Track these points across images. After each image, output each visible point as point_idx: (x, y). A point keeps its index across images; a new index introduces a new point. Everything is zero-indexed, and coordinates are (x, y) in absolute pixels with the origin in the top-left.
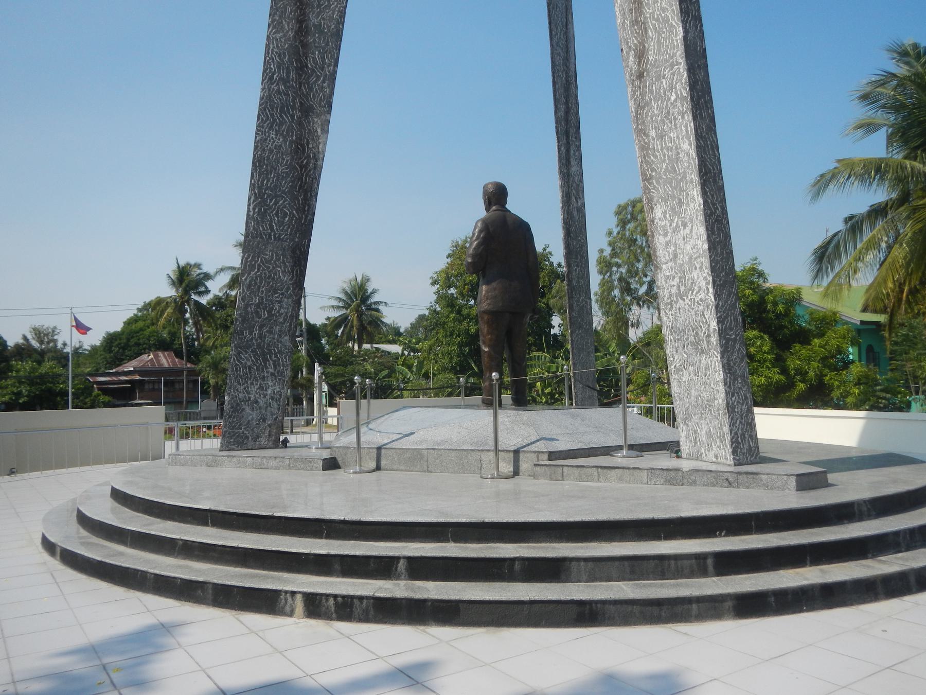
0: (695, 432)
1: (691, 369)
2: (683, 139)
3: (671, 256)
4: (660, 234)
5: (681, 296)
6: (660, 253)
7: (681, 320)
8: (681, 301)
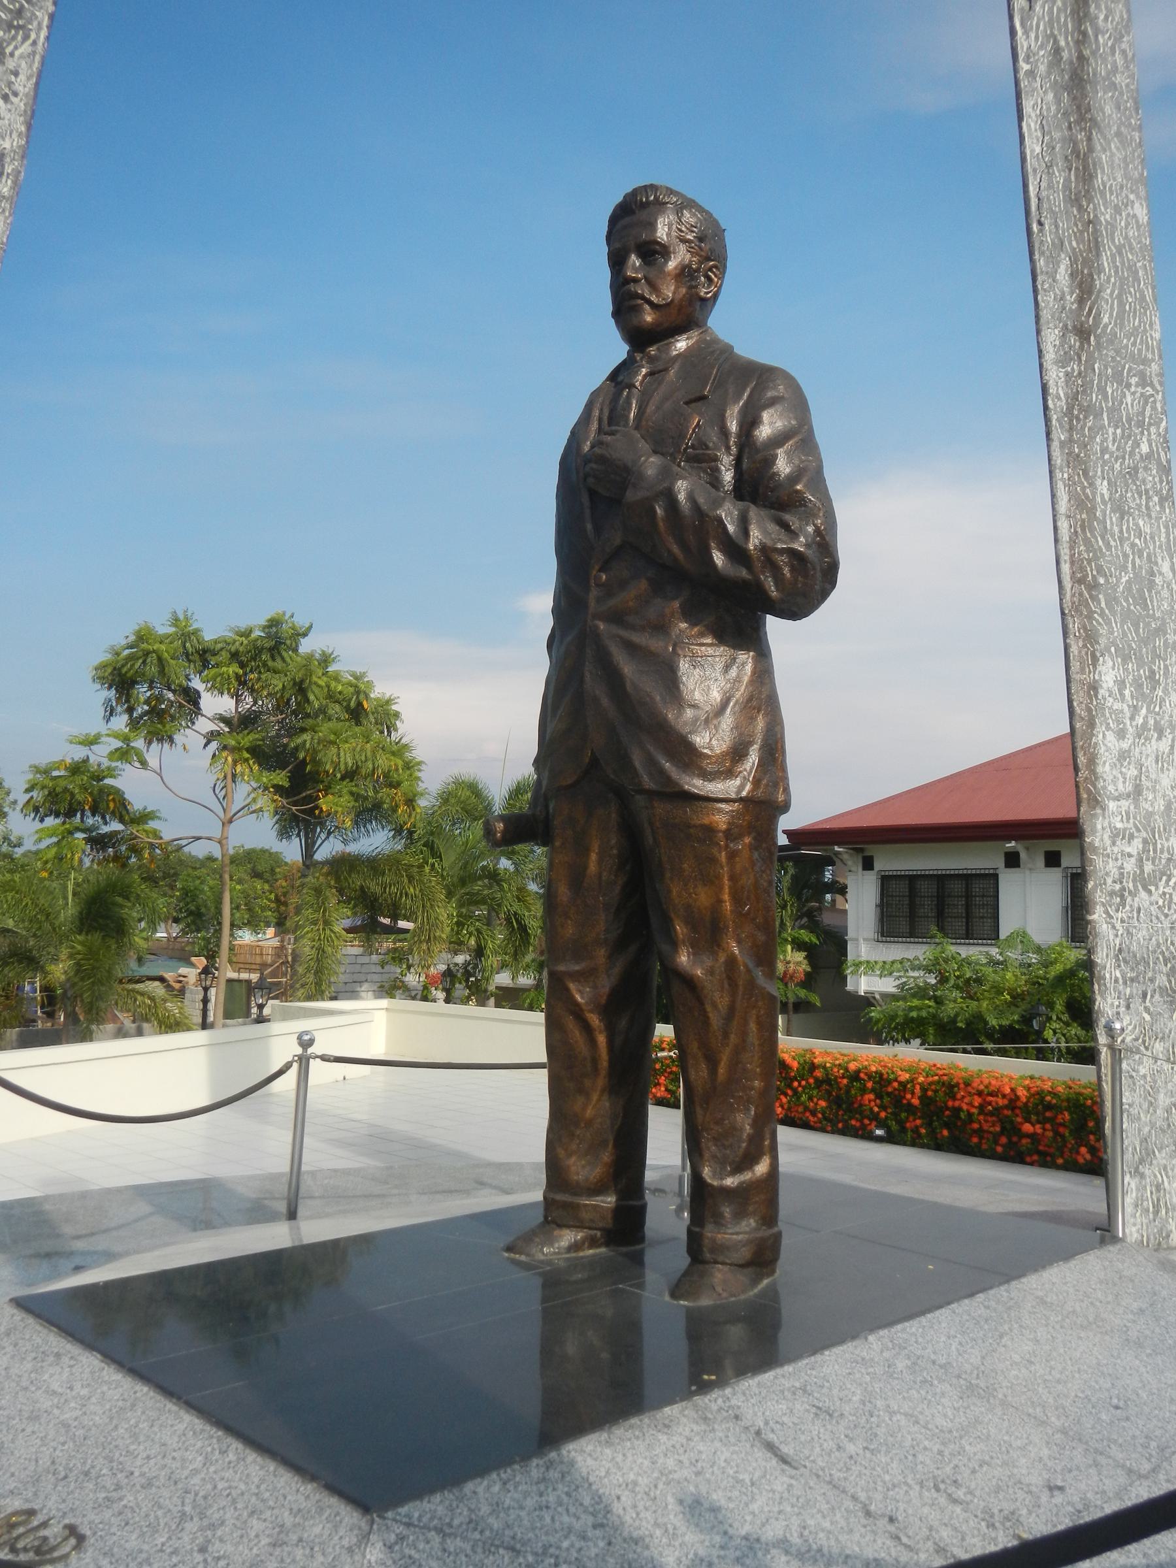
0: (1158, 1187)
1: (1158, 1047)
2: (1160, 547)
3: (1130, 788)
4: (1108, 728)
5: (1145, 882)
6: (1105, 768)
7: (1141, 935)
8: (1143, 894)
